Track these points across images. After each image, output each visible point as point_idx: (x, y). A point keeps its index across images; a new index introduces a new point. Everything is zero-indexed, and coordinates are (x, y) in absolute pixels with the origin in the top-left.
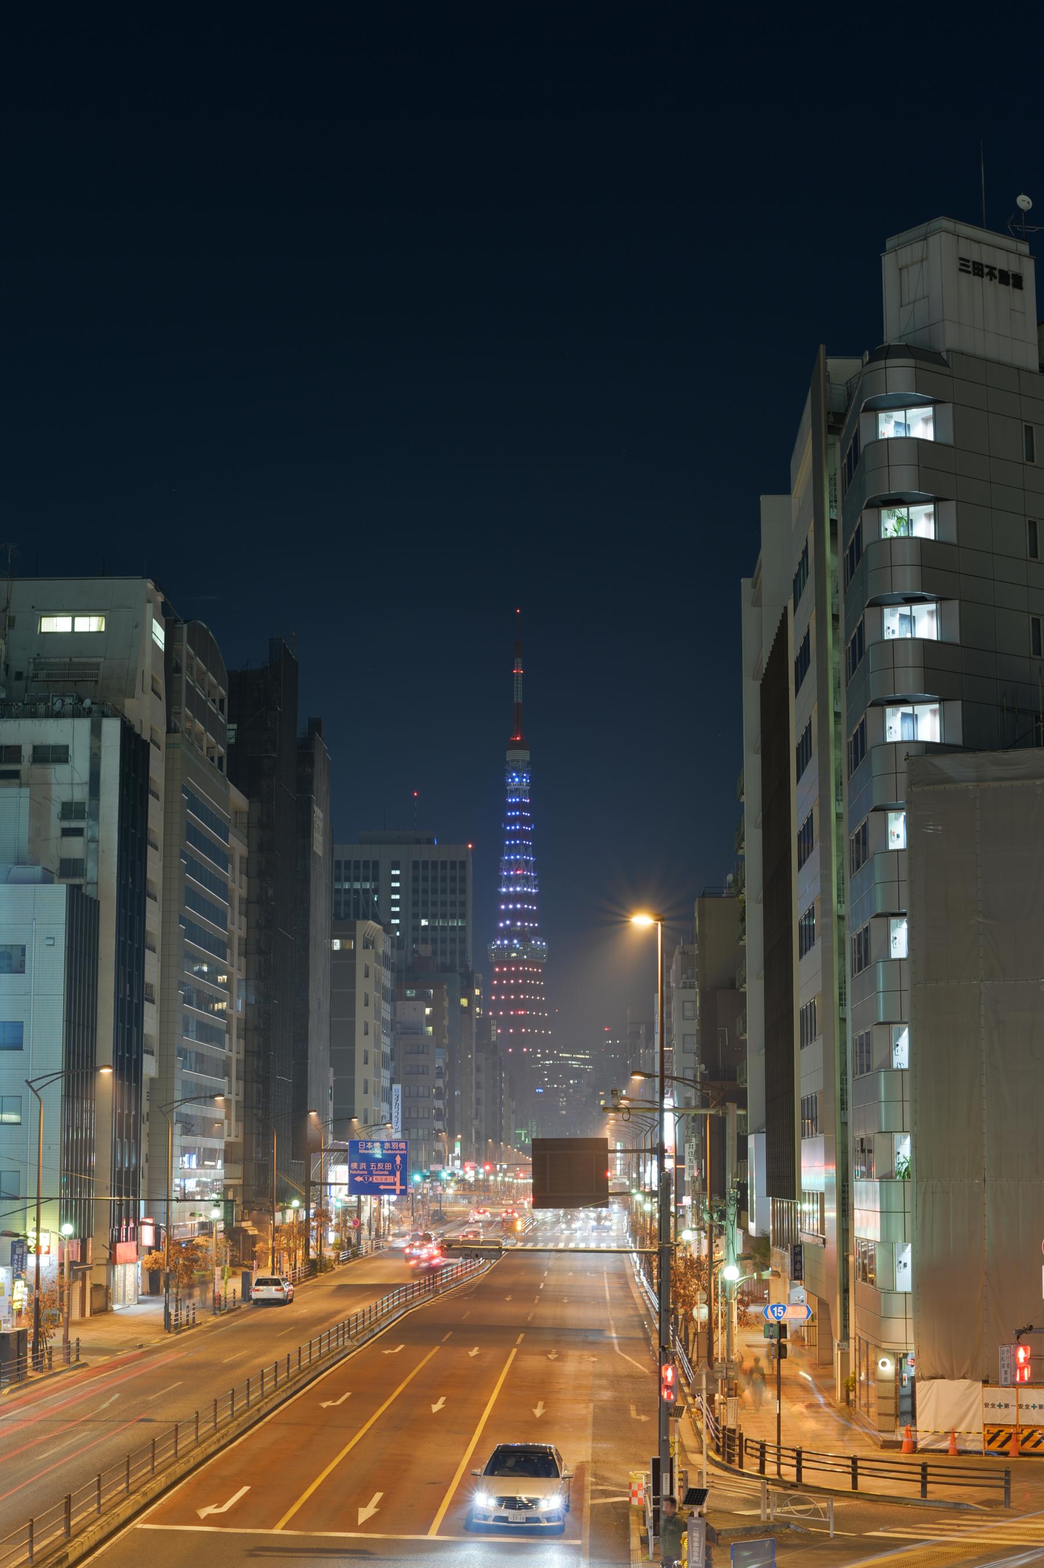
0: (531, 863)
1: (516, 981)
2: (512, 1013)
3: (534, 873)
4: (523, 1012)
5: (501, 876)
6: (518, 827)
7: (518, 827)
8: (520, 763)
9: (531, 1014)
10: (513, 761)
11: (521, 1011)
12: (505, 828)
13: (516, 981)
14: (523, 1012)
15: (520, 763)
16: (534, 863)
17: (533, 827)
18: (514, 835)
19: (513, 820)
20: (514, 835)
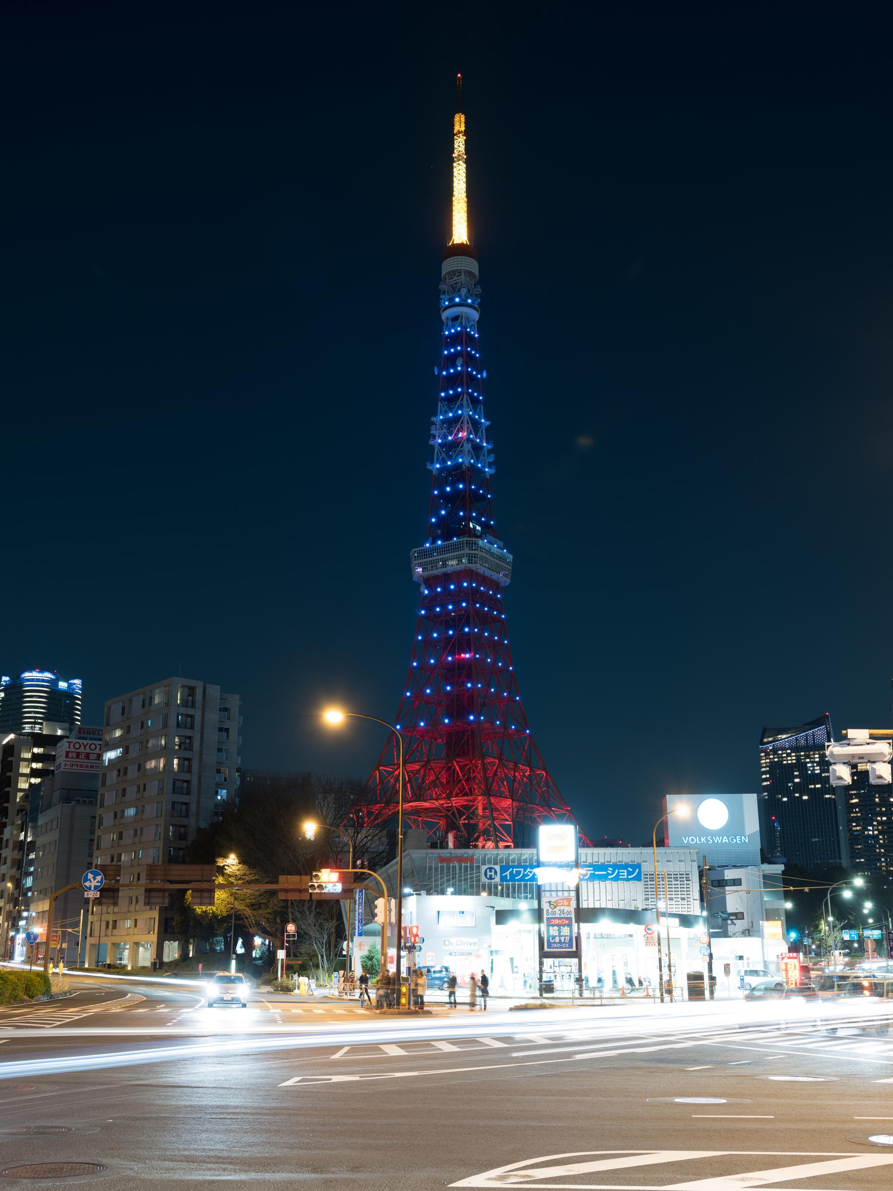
0: (483, 428)
1: (457, 604)
2: (450, 659)
3: (488, 442)
4: (468, 656)
5: (433, 447)
6: (459, 369)
7: (459, 369)
8: (463, 276)
9: (483, 660)
10: (453, 273)
11: (464, 653)
12: (440, 373)
13: (457, 604)
14: (468, 656)
15: (463, 276)
16: (488, 428)
17: (485, 375)
18: (452, 381)
19: (451, 360)
20: (452, 381)
